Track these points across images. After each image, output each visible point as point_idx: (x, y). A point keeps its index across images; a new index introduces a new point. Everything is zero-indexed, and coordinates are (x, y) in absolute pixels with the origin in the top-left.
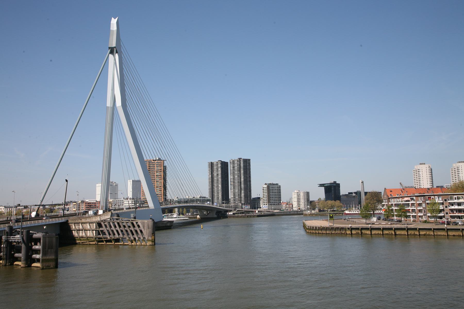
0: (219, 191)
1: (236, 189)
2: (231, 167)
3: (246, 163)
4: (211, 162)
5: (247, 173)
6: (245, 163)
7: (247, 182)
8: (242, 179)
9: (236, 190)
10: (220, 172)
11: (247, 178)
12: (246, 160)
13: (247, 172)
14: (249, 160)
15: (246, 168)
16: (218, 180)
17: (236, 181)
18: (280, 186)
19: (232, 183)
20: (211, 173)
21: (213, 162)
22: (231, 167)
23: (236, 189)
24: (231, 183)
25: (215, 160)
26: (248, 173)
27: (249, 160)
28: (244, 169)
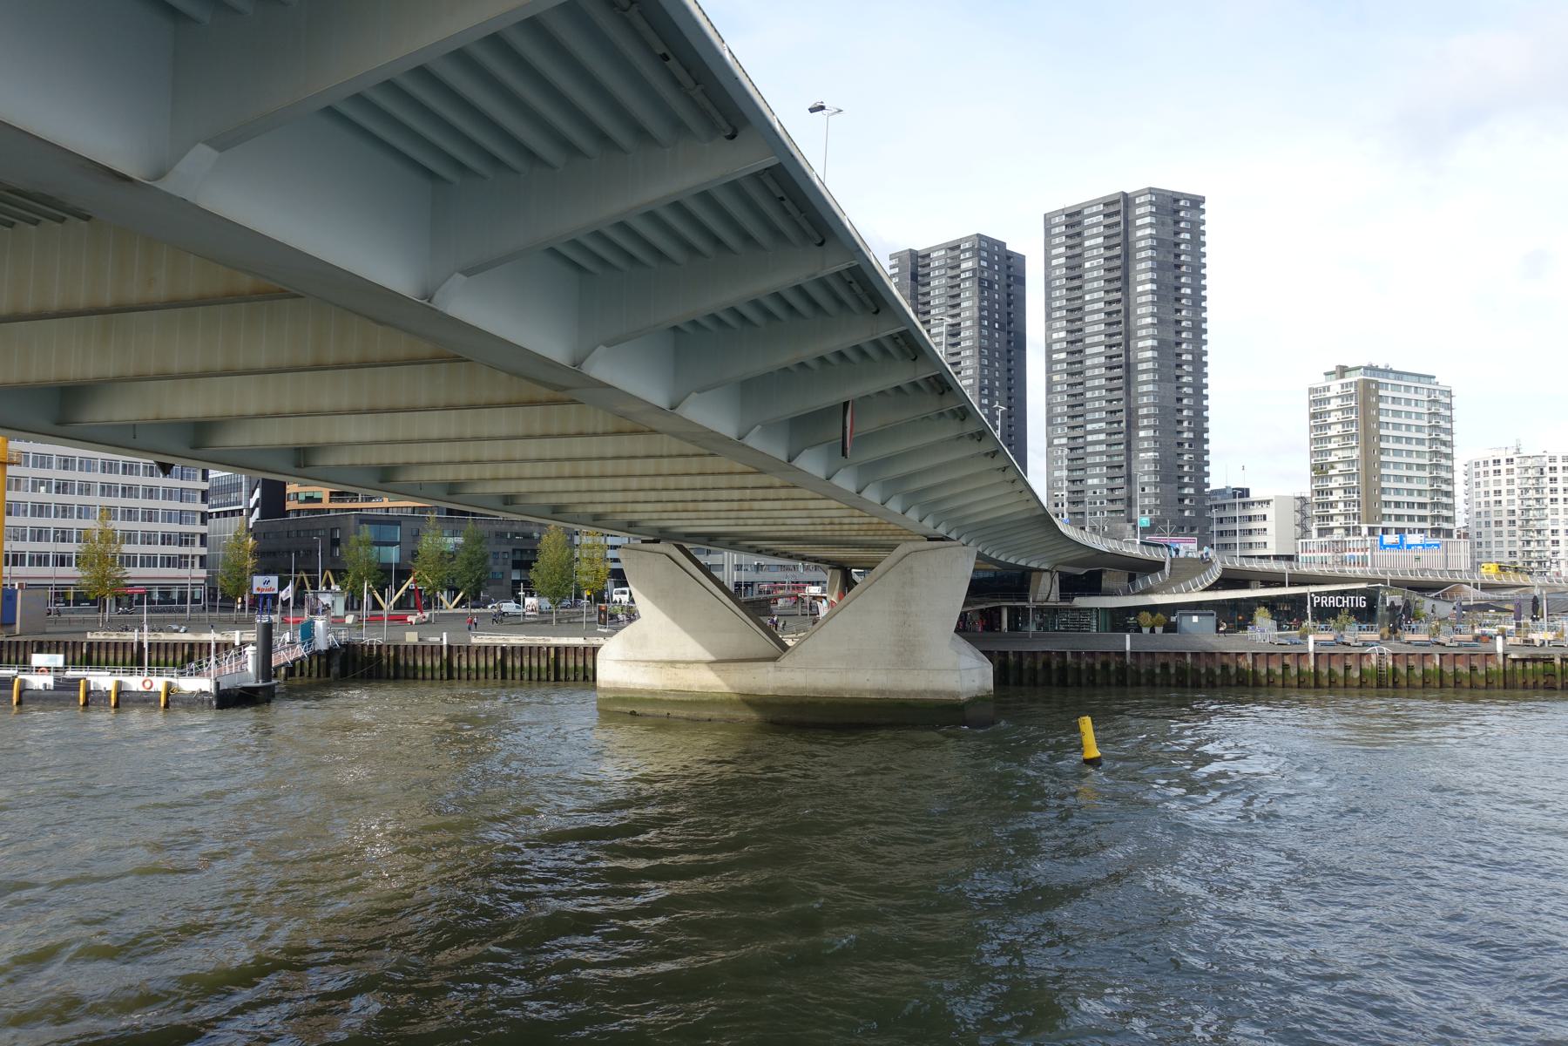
1: (1089, 417)
2: (1054, 262)
3: (1177, 223)
5: (1178, 300)
6: (1169, 220)
7: (1179, 366)
8: (1145, 348)
9: (1089, 427)
10: (969, 304)
11: (1178, 333)
12: (1176, 198)
13: (1178, 289)
14: (1196, 203)
15: (1171, 258)
17: (1095, 357)
18: (1449, 394)
19: (1056, 378)
21: (920, 246)
23: (1089, 417)
26: (1185, 296)
27: (1196, 203)
28: (1159, 267)
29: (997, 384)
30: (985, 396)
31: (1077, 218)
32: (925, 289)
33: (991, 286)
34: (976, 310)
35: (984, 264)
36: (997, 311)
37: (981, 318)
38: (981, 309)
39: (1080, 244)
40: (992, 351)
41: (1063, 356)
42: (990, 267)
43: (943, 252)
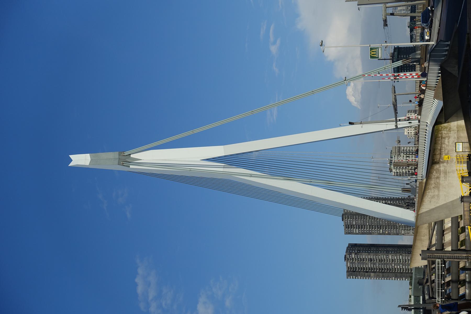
0: (401, 258)
2: (357, 232)
4: (348, 271)
16: (381, 261)
20: (366, 274)
21: (346, 270)
22: (357, 232)
24: (387, 234)
25: (343, 267)
29: (385, 249)
30: (389, 252)
31: (347, 226)
32: (357, 269)
33: (359, 250)
34: (366, 254)
35: (353, 251)
36: (366, 249)
37: (368, 252)
38: (365, 253)
39: (354, 225)
40: (376, 251)
41: (381, 231)
42: (354, 250)
43: (349, 263)
